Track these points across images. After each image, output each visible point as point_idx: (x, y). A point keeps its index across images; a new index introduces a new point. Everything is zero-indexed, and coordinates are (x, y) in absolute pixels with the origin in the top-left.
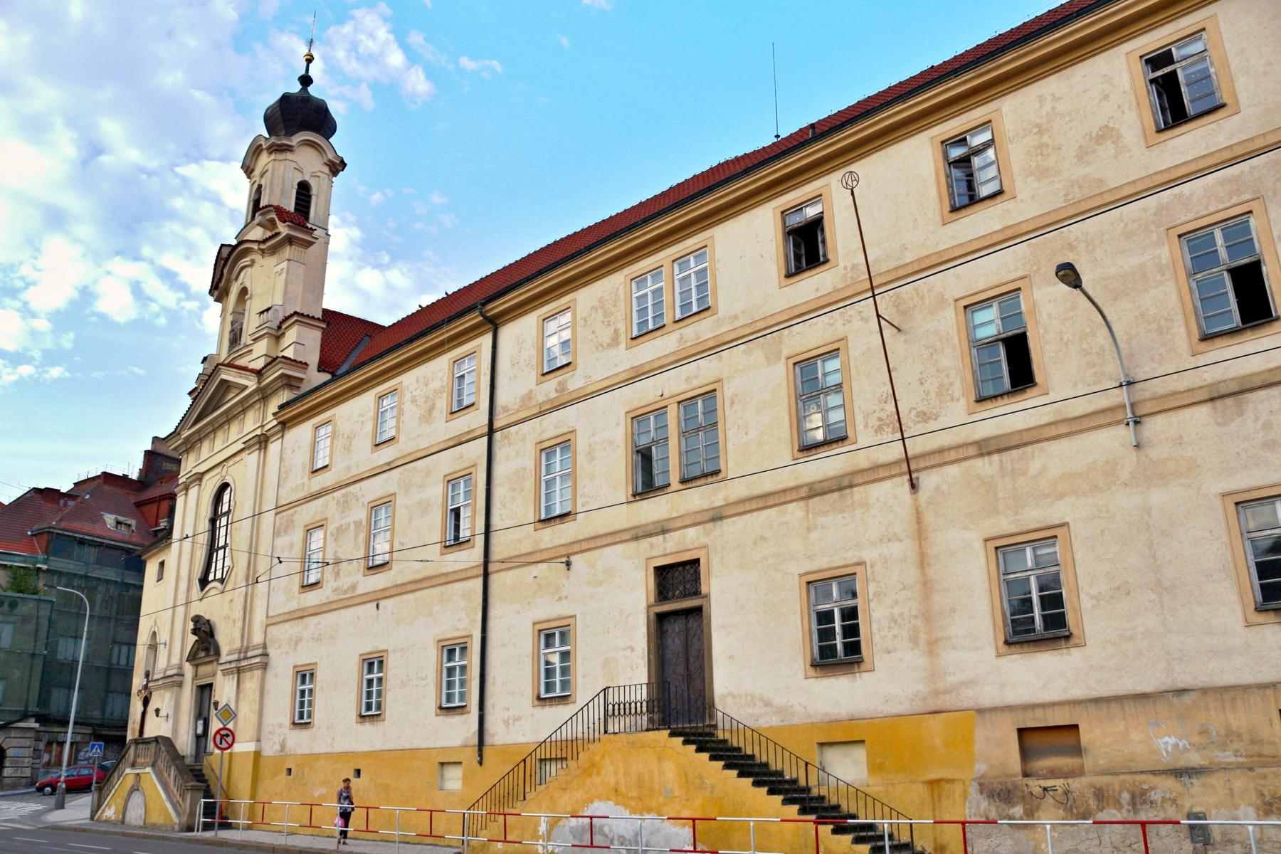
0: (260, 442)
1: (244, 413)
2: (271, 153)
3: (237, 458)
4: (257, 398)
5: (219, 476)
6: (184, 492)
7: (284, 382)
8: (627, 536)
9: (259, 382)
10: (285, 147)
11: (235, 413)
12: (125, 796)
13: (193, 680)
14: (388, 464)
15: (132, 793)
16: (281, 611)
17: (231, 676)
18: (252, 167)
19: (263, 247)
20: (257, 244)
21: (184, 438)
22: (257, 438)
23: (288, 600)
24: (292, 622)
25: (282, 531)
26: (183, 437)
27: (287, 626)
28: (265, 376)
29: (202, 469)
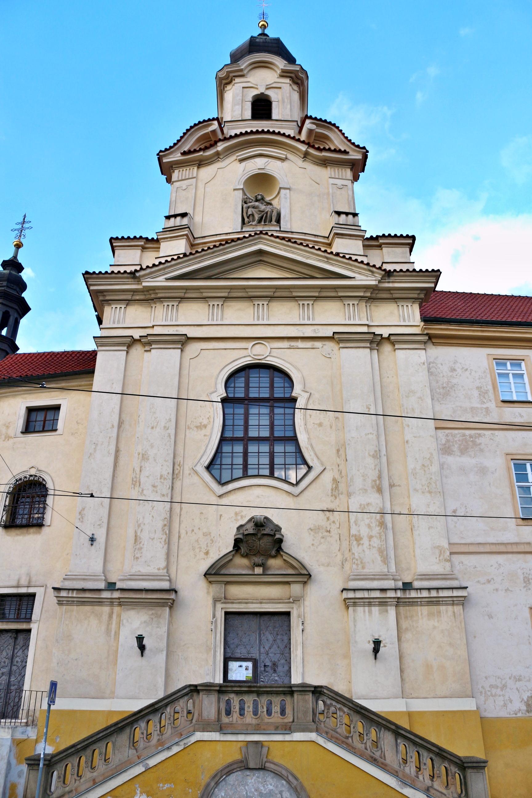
0: (371, 342)
1: (315, 301)
2: (282, 76)
3: (300, 344)
4: (361, 294)
5: (244, 353)
6: (125, 348)
7: (422, 296)
9: (380, 282)
10: (299, 82)
11: (295, 294)
12: (204, 779)
13: (216, 601)
15: (229, 773)
16: (480, 540)
18: (245, 72)
19: (311, 151)
20: (306, 147)
21: (144, 287)
22: (372, 336)
23: (492, 529)
24: (510, 556)
25: (455, 448)
26: (144, 284)
27: (500, 558)
28: (392, 279)
29: (192, 332)
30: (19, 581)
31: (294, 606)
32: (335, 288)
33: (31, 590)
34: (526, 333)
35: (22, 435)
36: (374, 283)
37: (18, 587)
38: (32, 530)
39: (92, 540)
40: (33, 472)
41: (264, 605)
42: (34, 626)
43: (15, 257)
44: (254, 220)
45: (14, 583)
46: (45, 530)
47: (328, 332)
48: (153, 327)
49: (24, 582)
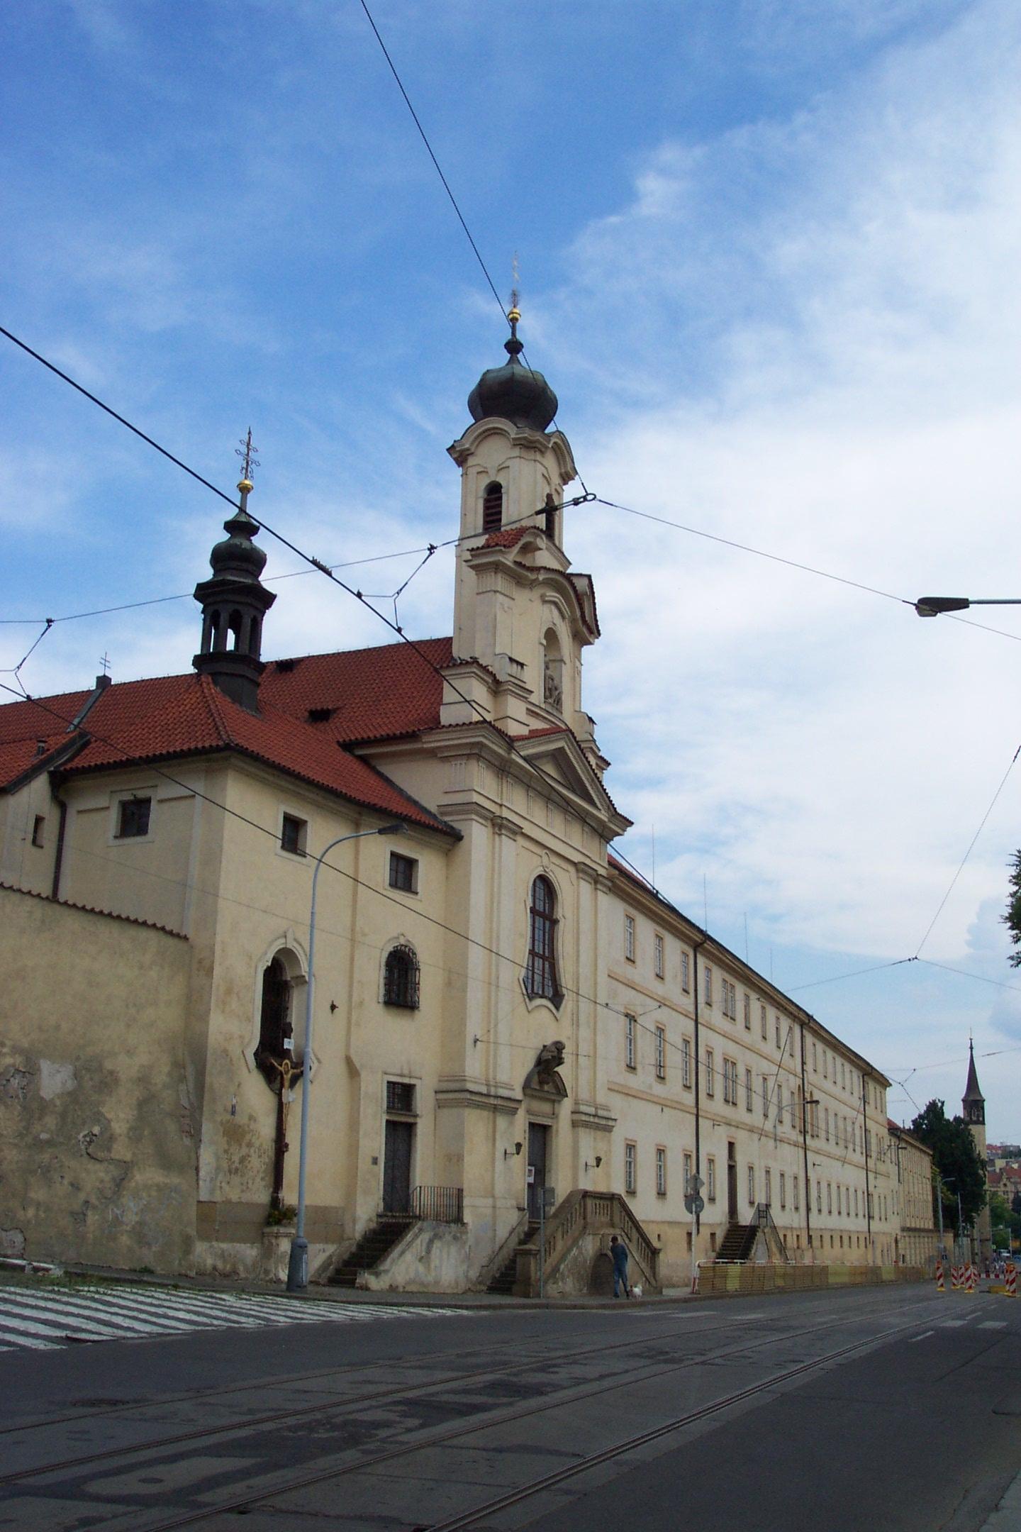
8: (748, 1128)
14: (664, 998)
17: (588, 1130)
30: (402, 1069)
31: (554, 1121)
32: (588, 813)
33: (413, 1081)
34: (645, 899)
35: (389, 888)
36: (606, 820)
37: (401, 1075)
38: (407, 1012)
39: (476, 1041)
40: (402, 941)
41: (545, 1119)
42: (419, 1120)
43: (242, 510)
44: (551, 697)
45: (399, 1072)
46: (416, 1012)
47: (577, 858)
48: (501, 805)
49: (406, 1072)
